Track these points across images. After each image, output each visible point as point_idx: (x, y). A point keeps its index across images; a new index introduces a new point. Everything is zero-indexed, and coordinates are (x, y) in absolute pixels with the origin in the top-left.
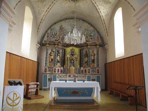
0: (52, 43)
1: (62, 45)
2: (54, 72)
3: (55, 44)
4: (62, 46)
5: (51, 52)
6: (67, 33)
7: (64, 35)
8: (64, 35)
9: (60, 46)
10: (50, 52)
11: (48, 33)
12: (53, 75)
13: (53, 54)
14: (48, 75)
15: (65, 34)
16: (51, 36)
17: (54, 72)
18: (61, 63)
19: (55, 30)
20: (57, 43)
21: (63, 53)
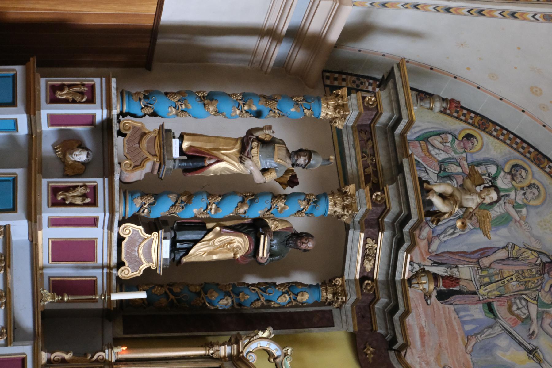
0: (382, 159)
1: (379, 274)
2: (55, 191)
3: (375, 188)
4: (363, 279)
5: (279, 152)
6: (521, 333)
7: (490, 308)
8: (490, 308)
9: (365, 256)
10: (282, 142)
11: (469, 137)
12: (20, 172)
13: (264, 171)
14: (23, 120)
15: (501, 310)
16: (453, 169)
17: (55, 191)
18: (170, 285)
19: (517, 207)
20: (394, 208)
21: (284, 300)
